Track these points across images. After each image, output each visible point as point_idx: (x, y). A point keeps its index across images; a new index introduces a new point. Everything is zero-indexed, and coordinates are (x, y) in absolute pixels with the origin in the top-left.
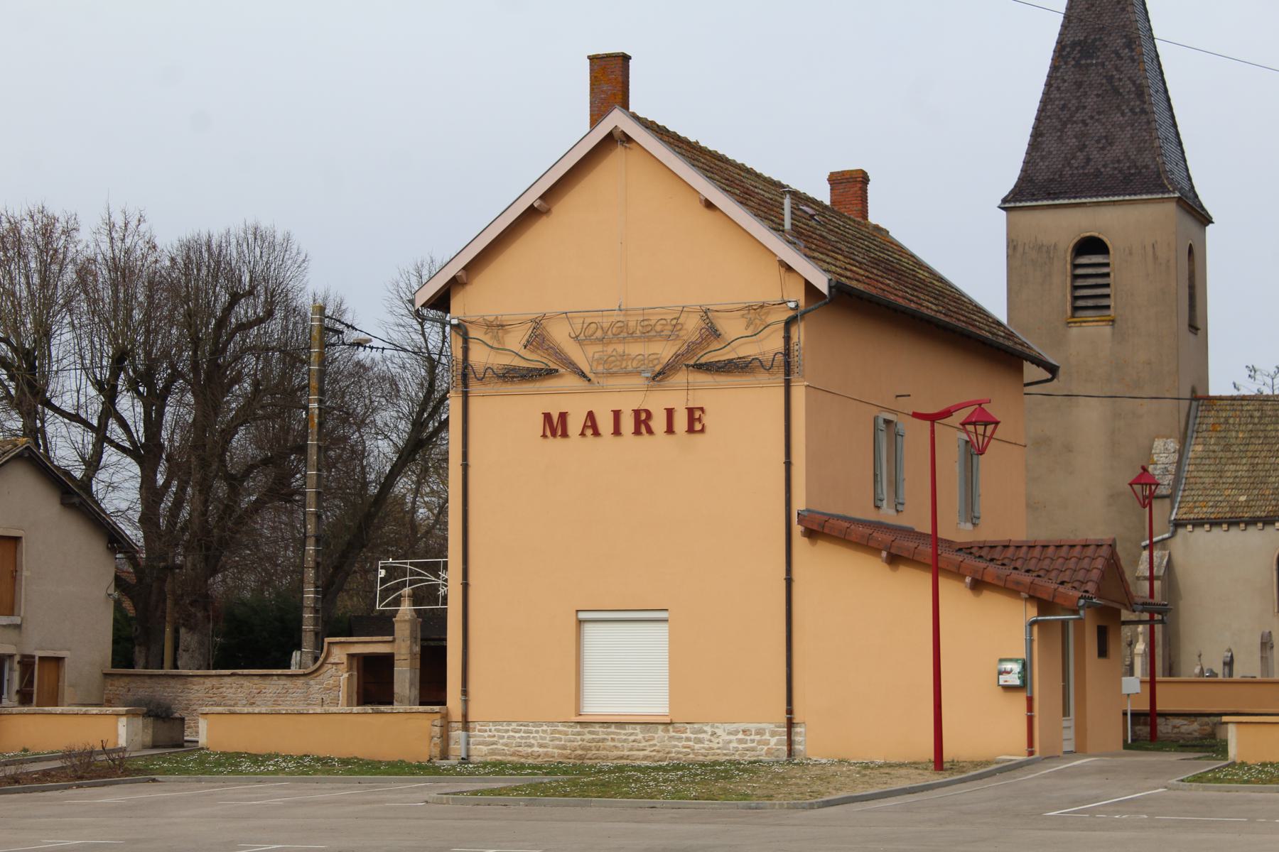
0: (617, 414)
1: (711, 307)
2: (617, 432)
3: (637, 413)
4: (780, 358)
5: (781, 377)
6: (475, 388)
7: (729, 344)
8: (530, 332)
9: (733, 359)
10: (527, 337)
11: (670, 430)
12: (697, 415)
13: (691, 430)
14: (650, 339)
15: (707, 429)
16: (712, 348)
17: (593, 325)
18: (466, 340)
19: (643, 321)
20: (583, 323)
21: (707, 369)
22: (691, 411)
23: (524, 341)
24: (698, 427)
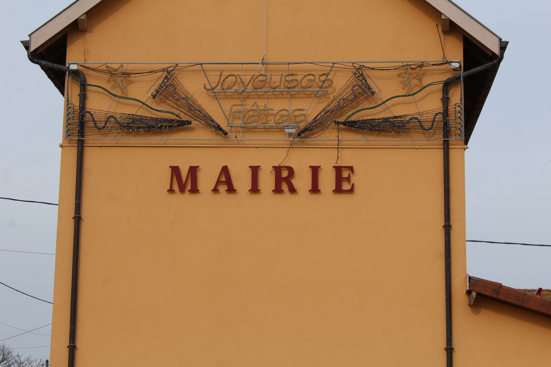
0: (255, 170)
1: (366, 65)
2: (255, 189)
3: (278, 170)
4: (439, 117)
5: (439, 138)
6: (91, 138)
7: (384, 103)
8: (160, 82)
9: (387, 118)
10: (156, 87)
11: (315, 189)
12: (345, 174)
13: (338, 190)
14: (292, 97)
15: (356, 190)
16: (361, 107)
17: (232, 79)
18: (84, 86)
19: (288, 75)
20: (221, 75)
21: (360, 127)
22: (338, 170)
23: (153, 91)
24: (346, 186)
